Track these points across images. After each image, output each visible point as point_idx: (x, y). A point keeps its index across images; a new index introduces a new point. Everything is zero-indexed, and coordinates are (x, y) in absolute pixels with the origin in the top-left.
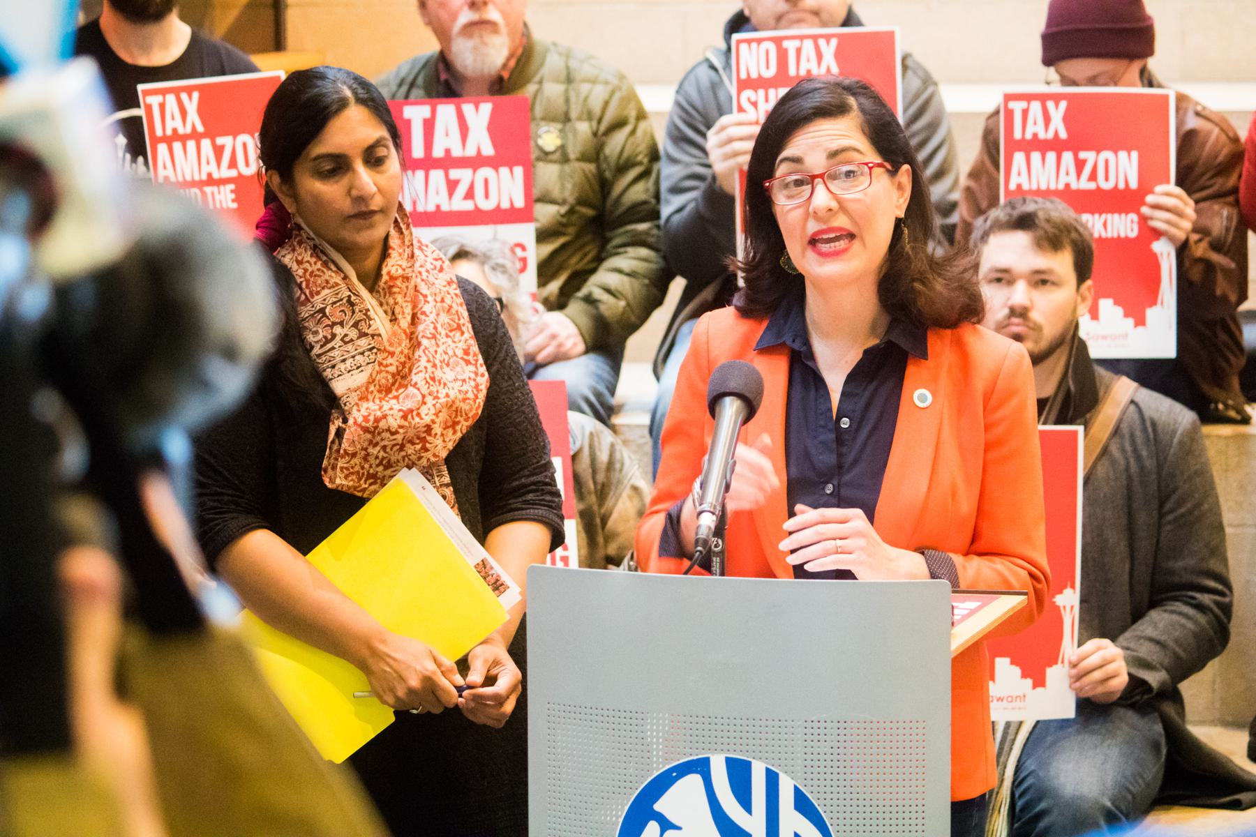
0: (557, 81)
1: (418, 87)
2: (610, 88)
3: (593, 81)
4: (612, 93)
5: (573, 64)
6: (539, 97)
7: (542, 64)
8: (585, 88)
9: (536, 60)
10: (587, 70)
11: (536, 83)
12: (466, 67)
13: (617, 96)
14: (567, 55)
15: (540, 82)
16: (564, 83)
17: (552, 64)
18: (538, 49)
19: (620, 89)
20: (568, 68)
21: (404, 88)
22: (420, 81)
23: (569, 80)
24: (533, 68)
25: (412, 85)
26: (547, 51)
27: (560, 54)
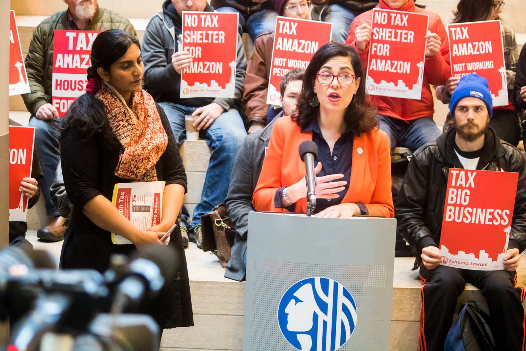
0: (108, 22)
1: (60, 23)
2: (126, 24)
3: (120, 22)
4: (127, 26)
5: (113, 16)
7: (103, 16)
8: (117, 24)
9: (100, 15)
10: (117, 18)
11: (101, 22)
12: (80, 16)
13: (128, 27)
14: (110, 13)
15: (102, 22)
16: (109, 23)
17: (105, 16)
18: (101, 11)
19: (129, 25)
20: (111, 18)
21: (55, 24)
22: (60, 20)
23: (112, 22)
24: (100, 17)
25: (57, 22)
26: (104, 11)
27: (108, 13)
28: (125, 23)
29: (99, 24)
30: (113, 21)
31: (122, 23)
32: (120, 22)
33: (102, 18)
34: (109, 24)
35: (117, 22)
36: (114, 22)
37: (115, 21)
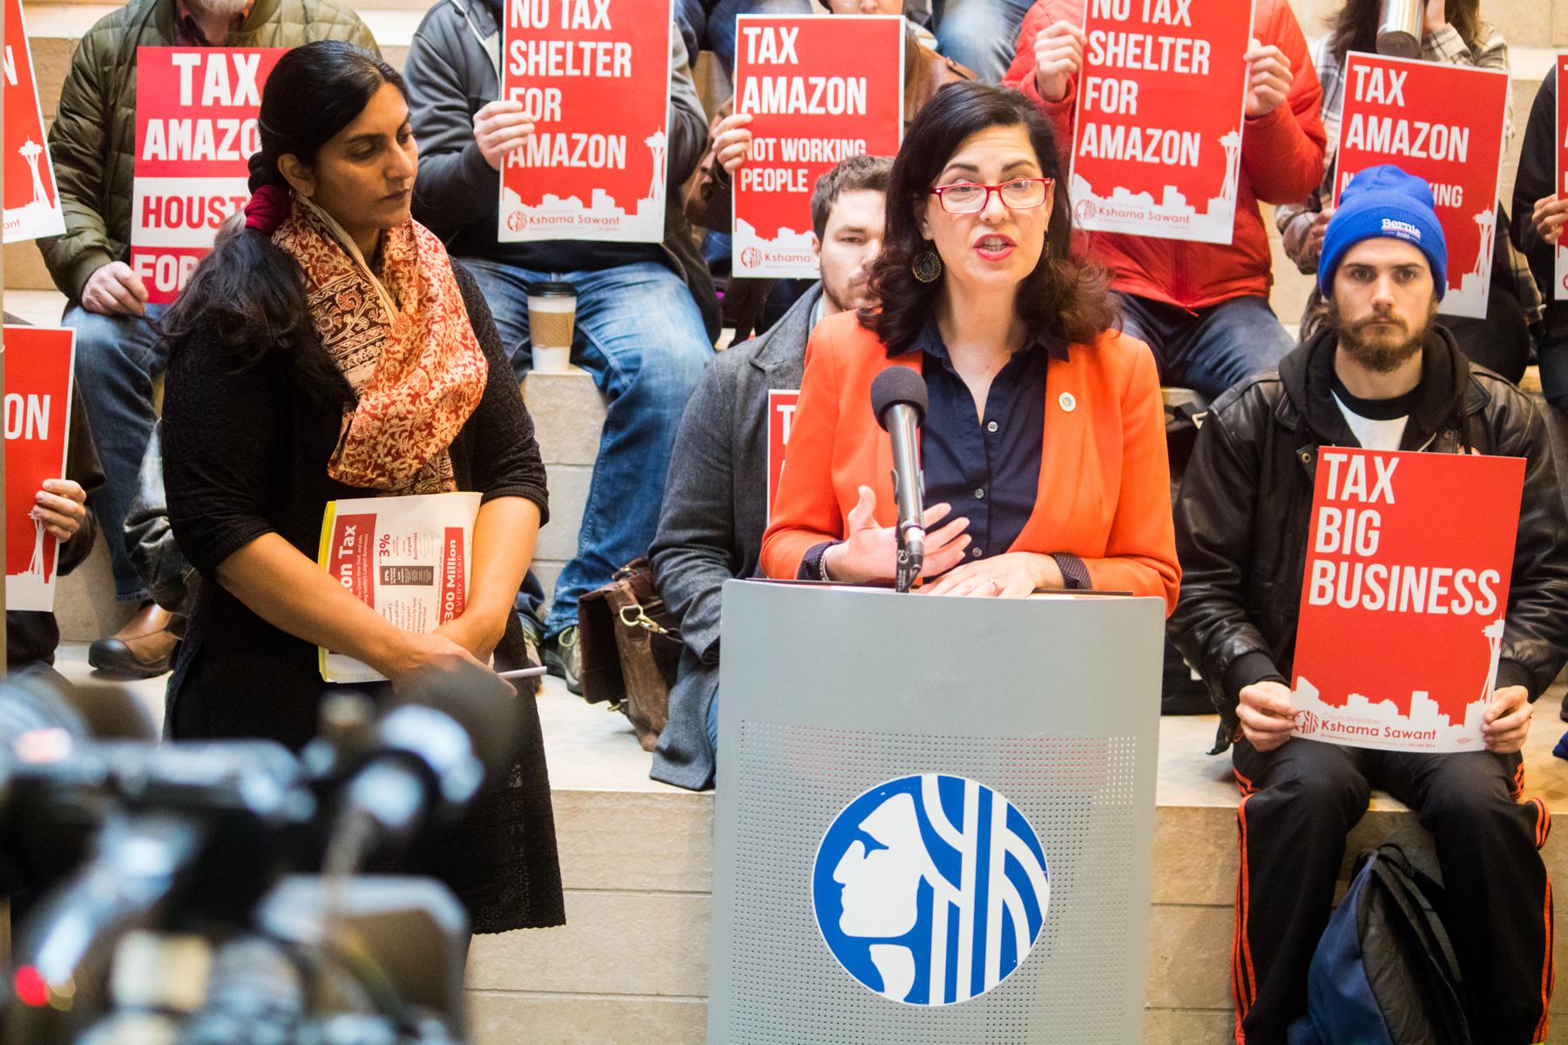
0: (294, 21)
1: (151, 27)
2: (349, 27)
3: (332, 21)
4: (351, 34)
6: (277, 36)
8: (324, 27)
10: (321, 10)
13: (357, 36)
15: (278, 21)
16: (300, 23)
19: (358, 28)
20: (304, 7)
21: (136, 29)
23: (307, 20)
25: (144, 24)
28: (345, 23)
29: (269, 27)
30: (309, 19)
31: (339, 23)
32: (332, 21)
33: (278, 10)
34: (302, 26)
35: (323, 21)
36: (313, 20)
37: (316, 19)
